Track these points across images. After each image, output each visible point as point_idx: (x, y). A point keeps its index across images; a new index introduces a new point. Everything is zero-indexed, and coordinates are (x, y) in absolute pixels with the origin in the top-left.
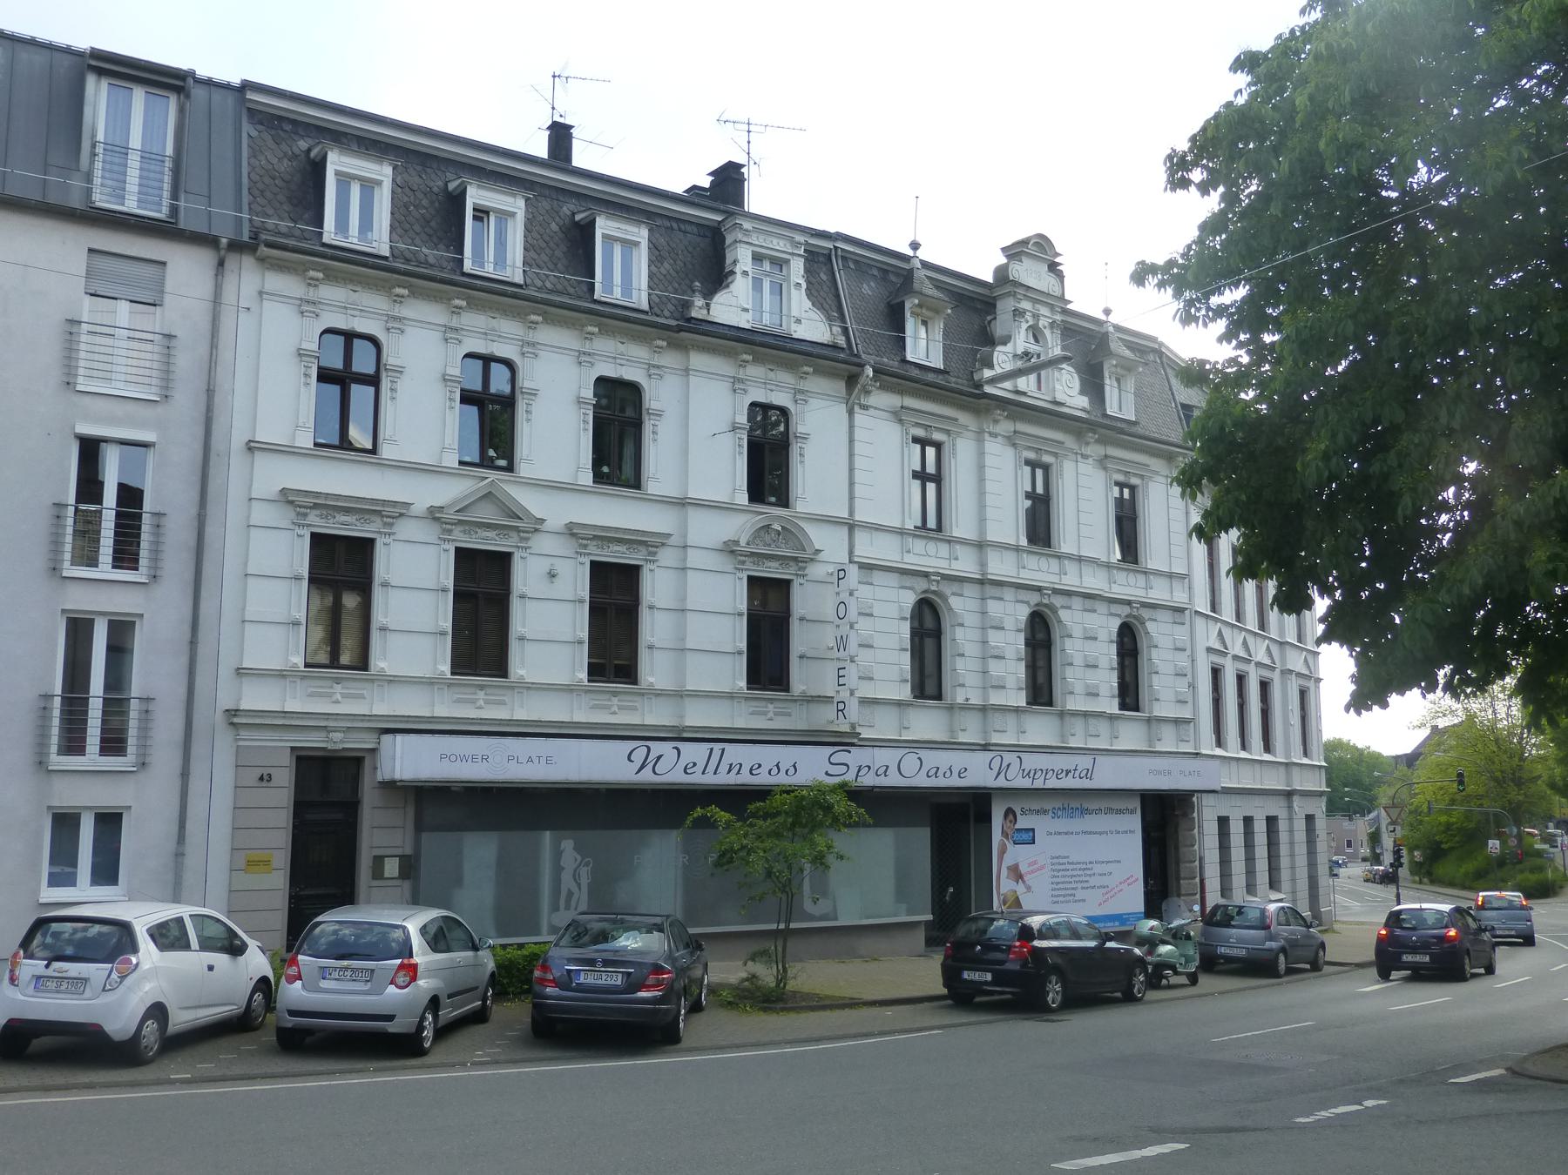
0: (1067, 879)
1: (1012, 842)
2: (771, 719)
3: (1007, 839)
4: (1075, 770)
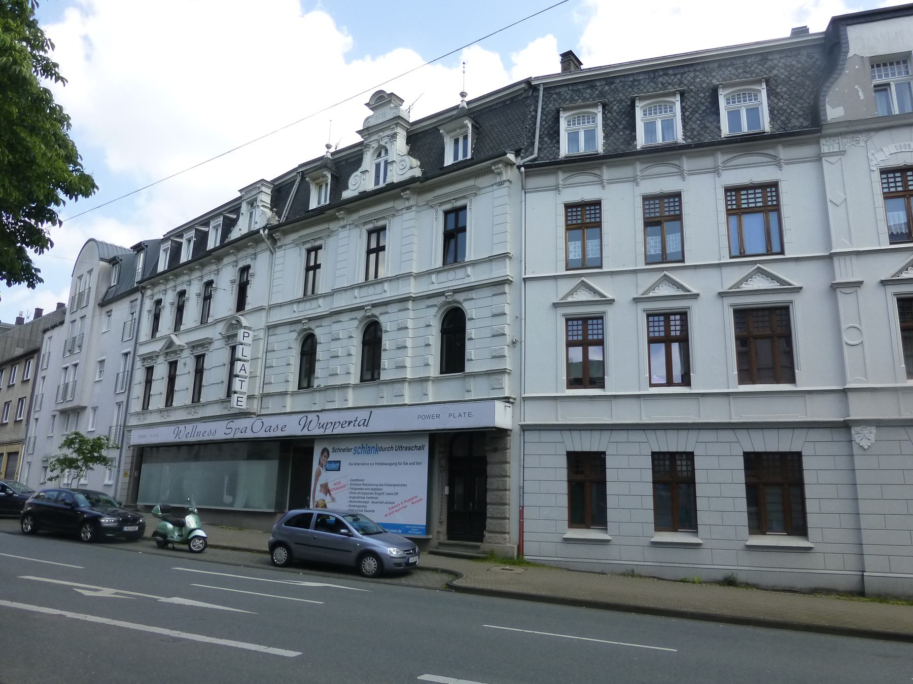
0: (360, 495)
2: (229, 410)
3: (322, 467)
4: (355, 421)
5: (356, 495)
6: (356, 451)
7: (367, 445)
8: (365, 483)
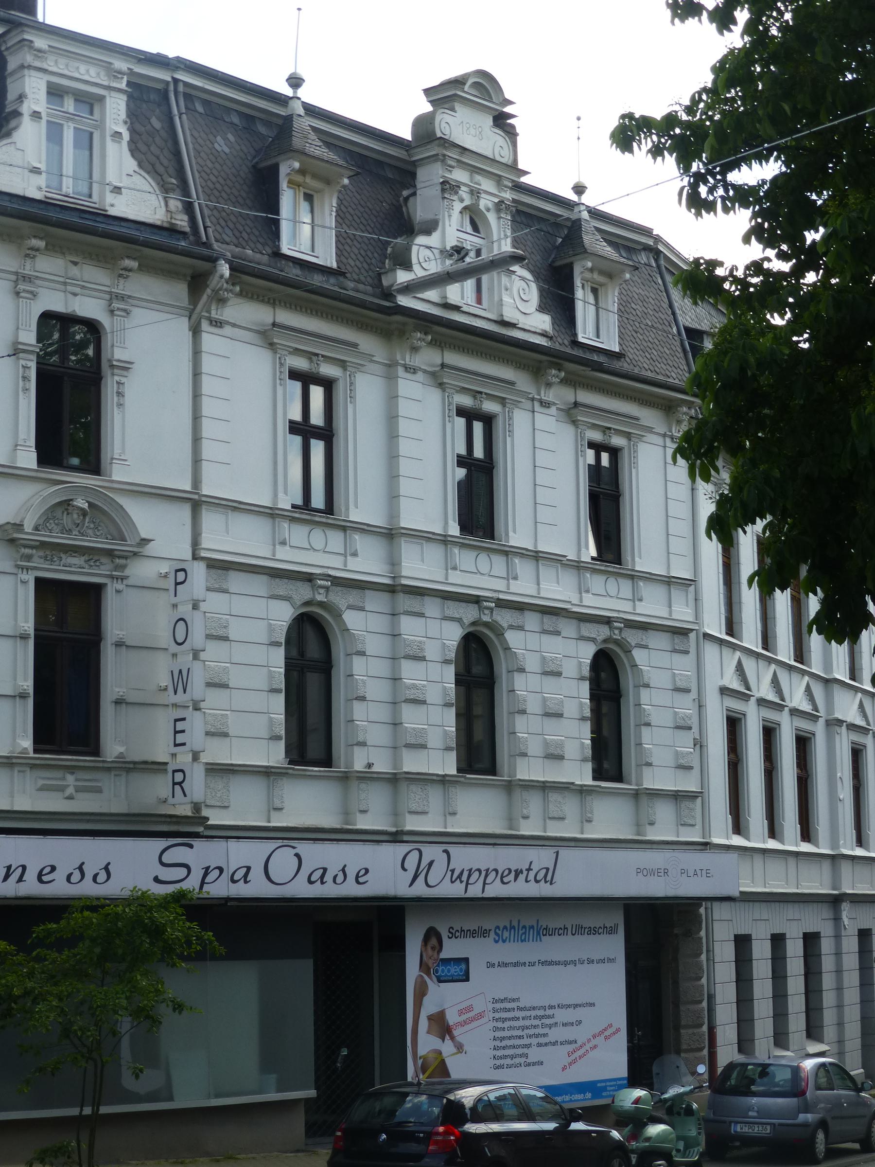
1: (435, 979)
2: (70, 798)
3: (428, 974)
4: (529, 870)
5: (507, 1033)
6: (452, 933)
7: (519, 921)
8: (522, 1005)
